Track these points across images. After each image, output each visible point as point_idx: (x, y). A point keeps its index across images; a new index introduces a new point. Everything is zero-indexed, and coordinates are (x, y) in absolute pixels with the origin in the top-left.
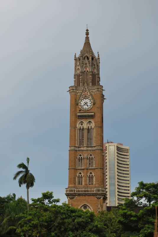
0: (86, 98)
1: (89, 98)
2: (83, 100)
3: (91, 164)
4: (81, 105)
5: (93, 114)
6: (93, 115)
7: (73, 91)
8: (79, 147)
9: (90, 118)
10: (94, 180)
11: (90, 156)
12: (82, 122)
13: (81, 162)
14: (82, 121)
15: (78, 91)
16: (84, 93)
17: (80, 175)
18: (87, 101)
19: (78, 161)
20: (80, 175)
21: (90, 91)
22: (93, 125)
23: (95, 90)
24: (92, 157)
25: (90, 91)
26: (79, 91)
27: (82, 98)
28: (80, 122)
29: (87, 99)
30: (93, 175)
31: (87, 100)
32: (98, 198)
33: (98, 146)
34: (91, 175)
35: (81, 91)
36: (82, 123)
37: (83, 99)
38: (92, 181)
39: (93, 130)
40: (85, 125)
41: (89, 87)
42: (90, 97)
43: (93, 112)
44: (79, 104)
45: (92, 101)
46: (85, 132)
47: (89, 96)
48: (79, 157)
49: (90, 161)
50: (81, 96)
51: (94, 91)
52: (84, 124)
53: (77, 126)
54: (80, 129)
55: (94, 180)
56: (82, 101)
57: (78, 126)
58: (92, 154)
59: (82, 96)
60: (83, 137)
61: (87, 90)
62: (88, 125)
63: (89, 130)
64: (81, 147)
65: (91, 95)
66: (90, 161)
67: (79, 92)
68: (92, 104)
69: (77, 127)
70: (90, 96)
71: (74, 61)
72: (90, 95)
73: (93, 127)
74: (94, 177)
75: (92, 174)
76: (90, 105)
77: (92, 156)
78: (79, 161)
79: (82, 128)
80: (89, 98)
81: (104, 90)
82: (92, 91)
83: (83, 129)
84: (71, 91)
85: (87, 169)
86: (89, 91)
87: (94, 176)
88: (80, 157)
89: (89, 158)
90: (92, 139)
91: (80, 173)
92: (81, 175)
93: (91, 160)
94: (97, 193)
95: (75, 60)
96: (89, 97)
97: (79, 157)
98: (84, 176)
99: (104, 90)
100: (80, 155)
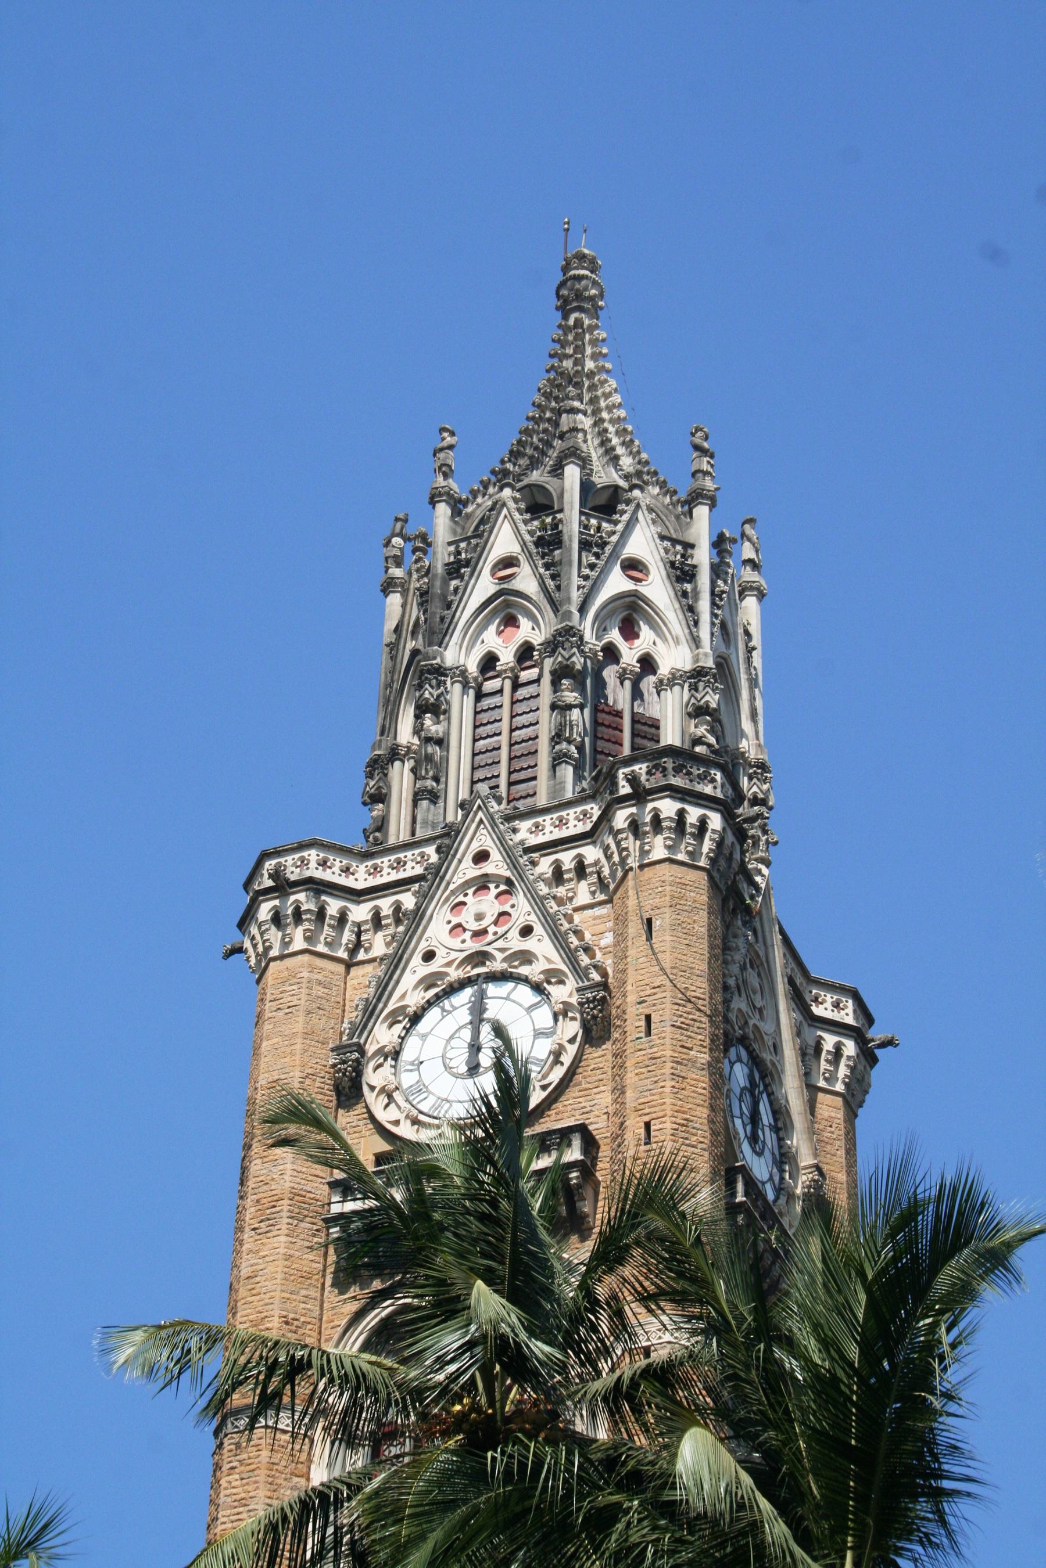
1: (524, 970)
2: (435, 1013)
4: (408, 1079)
5: (574, 1154)
15: (360, 912)
25: (545, 865)
26: (385, 905)
35: (408, 900)
41: (525, 825)
44: (375, 1077)
50: (395, 962)
51: (591, 853)
56: (422, 1026)
67: (377, 921)
68: (572, 1028)
70: (538, 929)
72: (533, 920)
82: (567, 858)
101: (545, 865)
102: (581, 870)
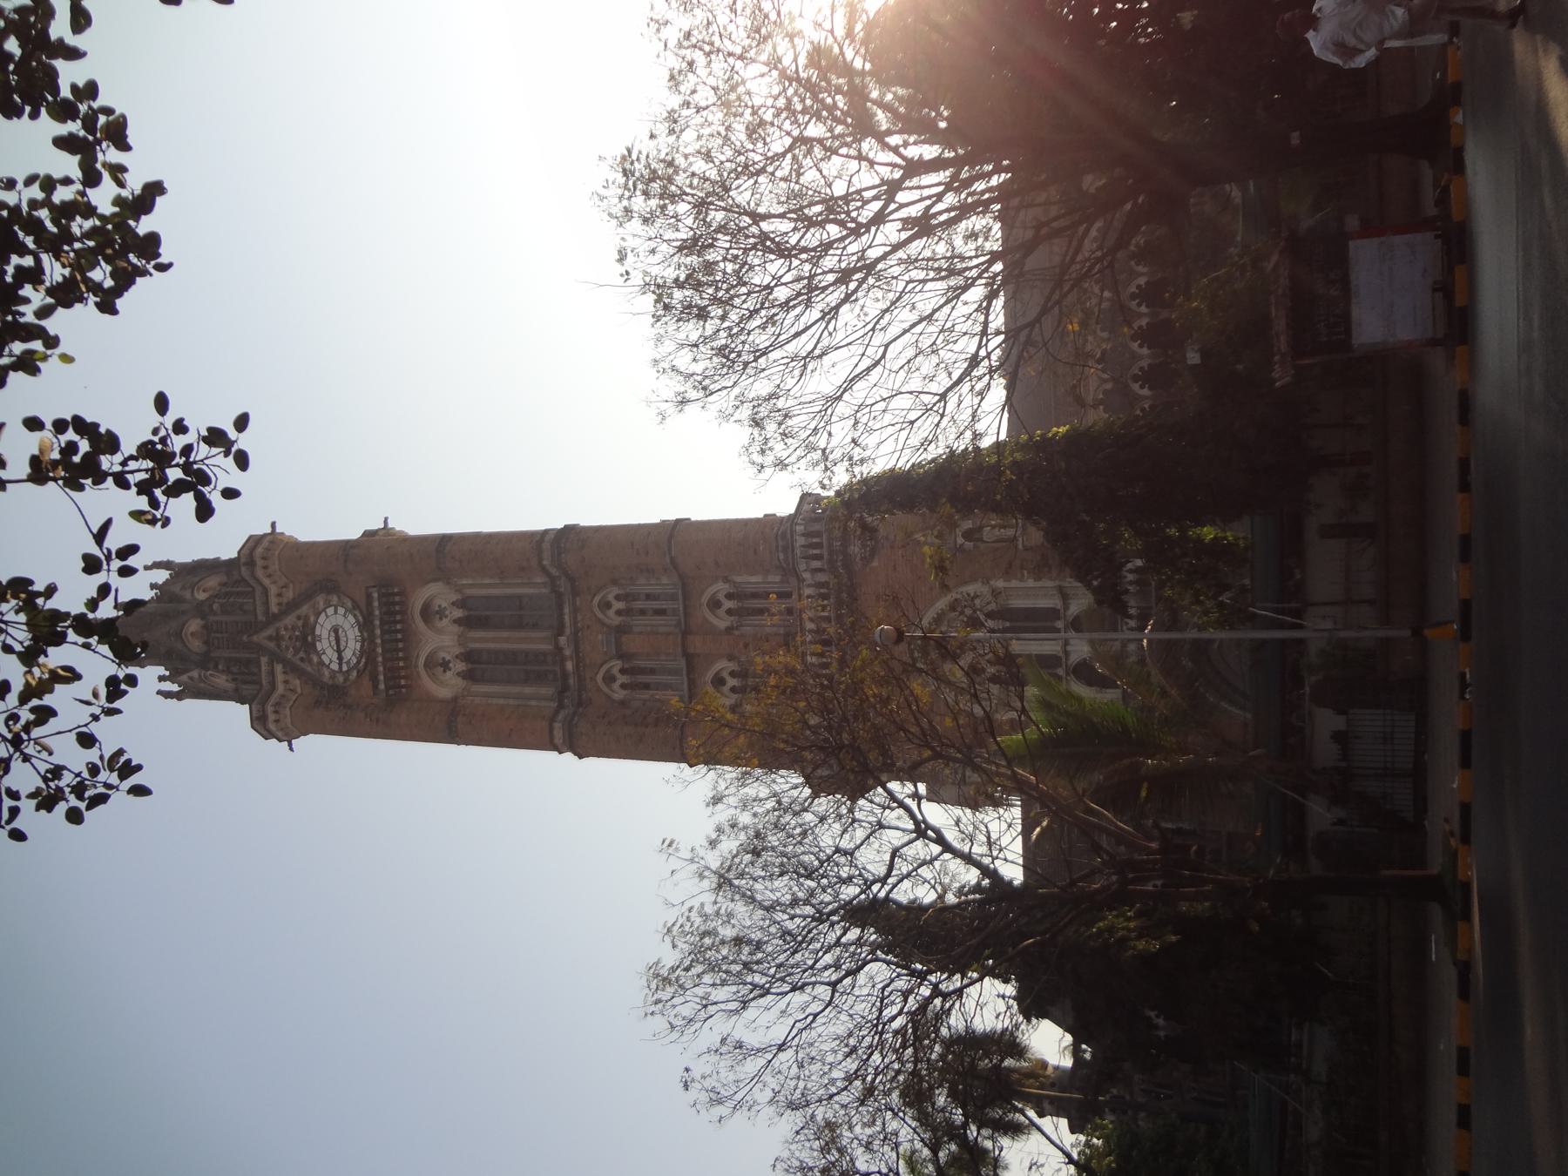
0: (306, 640)
3: (656, 605)
6: (381, 596)
7: (272, 717)
8: (564, 689)
9: (403, 612)
10: (753, 579)
11: (611, 613)
12: (426, 665)
13: (652, 671)
14: (422, 661)
15: (281, 688)
16: (287, 648)
17: (732, 682)
18: (325, 634)
19: (646, 695)
20: (732, 682)
21: (274, 609)
22: (439, 594)
23: (266, 582)
24: (618, 598)
26: (280, 677)
27: (310, 661)
28: (433, 677)
29: (318, 632)
30: (720, 588)
31: (323, 628)
32: (873, 552)
33: (540, 560)
34: (728, 604)
35: (279, 668)
36: (437, 664)
37: (315, 659)
38: (766, 595)
39: (469, 592)
40: (441, 640)
42: (304, 609)
43: (369, 596)
45: (320, 600)
46: (485, 640)
47: (299, 618)
48: (623, 686)
49: (643, 612)
51: (273, 590)
52: (442, 654)
53: (444, 693)
54: (469, 676)
55: (753, 579)
57: (447, 686)
58: (597, 599)
59: (302, 660)
60: (511, 657)
61: (270, 631)
62: (445, 621)
63: (471, 621)
64: (565, 676)
65: (293, 605)
66: (643, 612)
67: (286, 682)
68: (335, 599)
69: (455, 699)
70: (298, 612)
71: (189, 703)
73: (454, 597)
74: (739, 579)
75: (721, 597)
76: (341, 611)
77: (611, 598)
78: (647, 686)
79: (461, 666)
80: (312, 619)
81: (273, 525)
82: (273, 601)
83: (468, 656)
84: (272, 727)
85: (686, 633)
86: (276, 618)
87: (726, 580)
88: (622, 679)
89: (617, 620)
90: (520, 597)
91: (719, 681)
92: (732, 674)
93: (639, 605)
94: (831, 553)
95: (178, 696)
96: (307, 617)
97: (623, 686)
98: (731, 658)
99: (273, 525)
100: (609, 679)
101: (274, 609)
102: (279, 595)
